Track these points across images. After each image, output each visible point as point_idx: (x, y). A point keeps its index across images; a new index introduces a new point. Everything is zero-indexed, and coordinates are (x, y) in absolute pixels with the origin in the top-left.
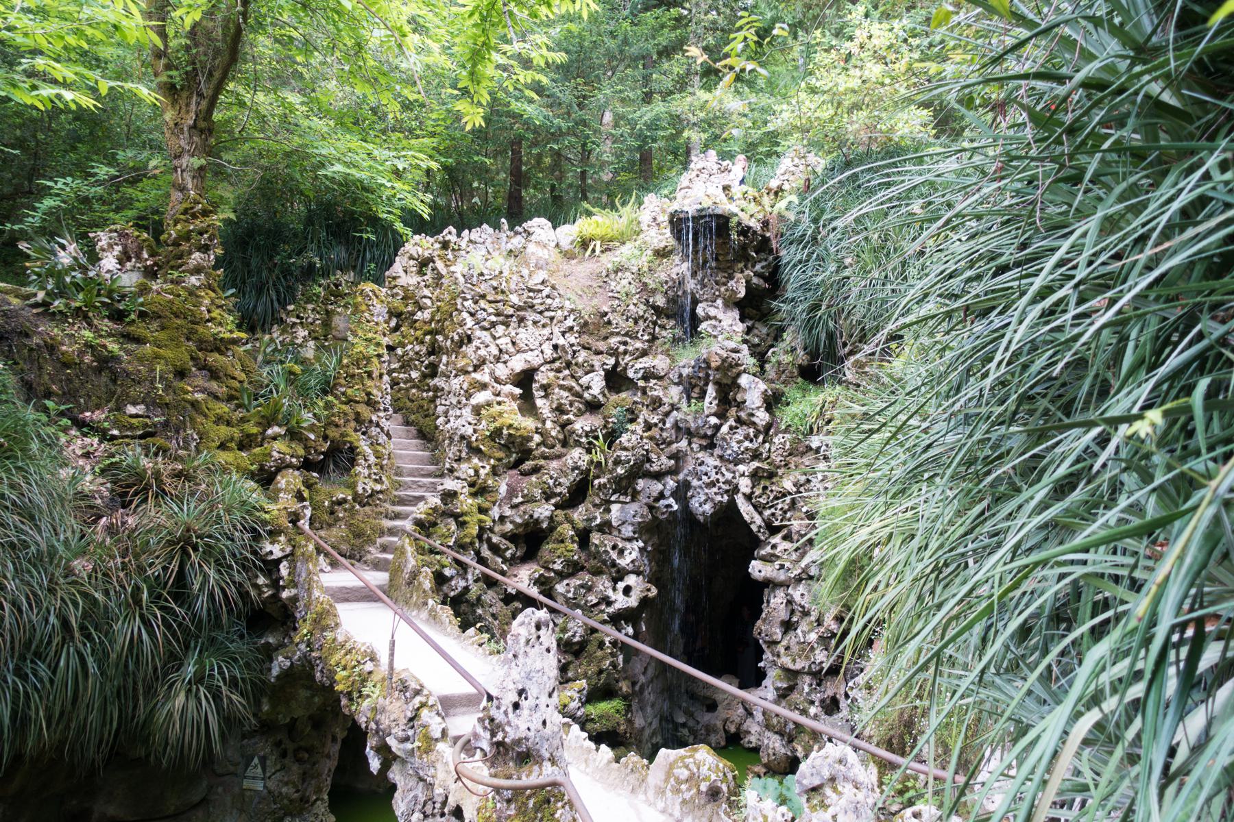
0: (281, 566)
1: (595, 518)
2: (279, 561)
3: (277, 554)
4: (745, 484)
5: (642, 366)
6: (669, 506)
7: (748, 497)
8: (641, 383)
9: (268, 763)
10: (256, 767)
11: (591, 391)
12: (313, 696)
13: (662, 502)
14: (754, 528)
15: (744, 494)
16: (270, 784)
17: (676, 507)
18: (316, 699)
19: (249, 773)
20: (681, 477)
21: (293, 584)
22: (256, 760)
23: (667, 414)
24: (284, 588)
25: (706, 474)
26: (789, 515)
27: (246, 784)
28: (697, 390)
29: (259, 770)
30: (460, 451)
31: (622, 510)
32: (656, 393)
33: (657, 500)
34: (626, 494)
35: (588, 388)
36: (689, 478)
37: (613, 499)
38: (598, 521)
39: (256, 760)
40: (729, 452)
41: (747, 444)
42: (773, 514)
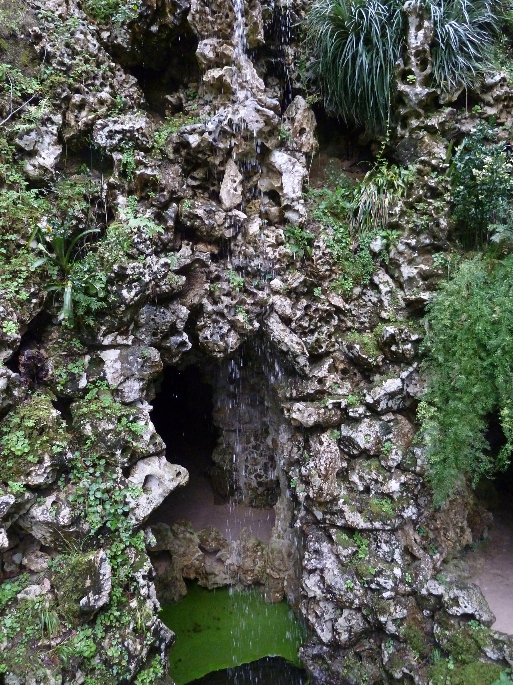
4: (283, 305)
6: (183, 344)
7: (286, 320)
11: (38, 161)
13: (175, 339)
17: (190, 345)
20: (193, 298)
23: (165, 206)
25: (227, 295)
26: (333, 340)
28: (199, 174)
31: (122, 358)
32: (149, 172)
35: (33, 154)
36: (205, 301)
42: (317, 340)
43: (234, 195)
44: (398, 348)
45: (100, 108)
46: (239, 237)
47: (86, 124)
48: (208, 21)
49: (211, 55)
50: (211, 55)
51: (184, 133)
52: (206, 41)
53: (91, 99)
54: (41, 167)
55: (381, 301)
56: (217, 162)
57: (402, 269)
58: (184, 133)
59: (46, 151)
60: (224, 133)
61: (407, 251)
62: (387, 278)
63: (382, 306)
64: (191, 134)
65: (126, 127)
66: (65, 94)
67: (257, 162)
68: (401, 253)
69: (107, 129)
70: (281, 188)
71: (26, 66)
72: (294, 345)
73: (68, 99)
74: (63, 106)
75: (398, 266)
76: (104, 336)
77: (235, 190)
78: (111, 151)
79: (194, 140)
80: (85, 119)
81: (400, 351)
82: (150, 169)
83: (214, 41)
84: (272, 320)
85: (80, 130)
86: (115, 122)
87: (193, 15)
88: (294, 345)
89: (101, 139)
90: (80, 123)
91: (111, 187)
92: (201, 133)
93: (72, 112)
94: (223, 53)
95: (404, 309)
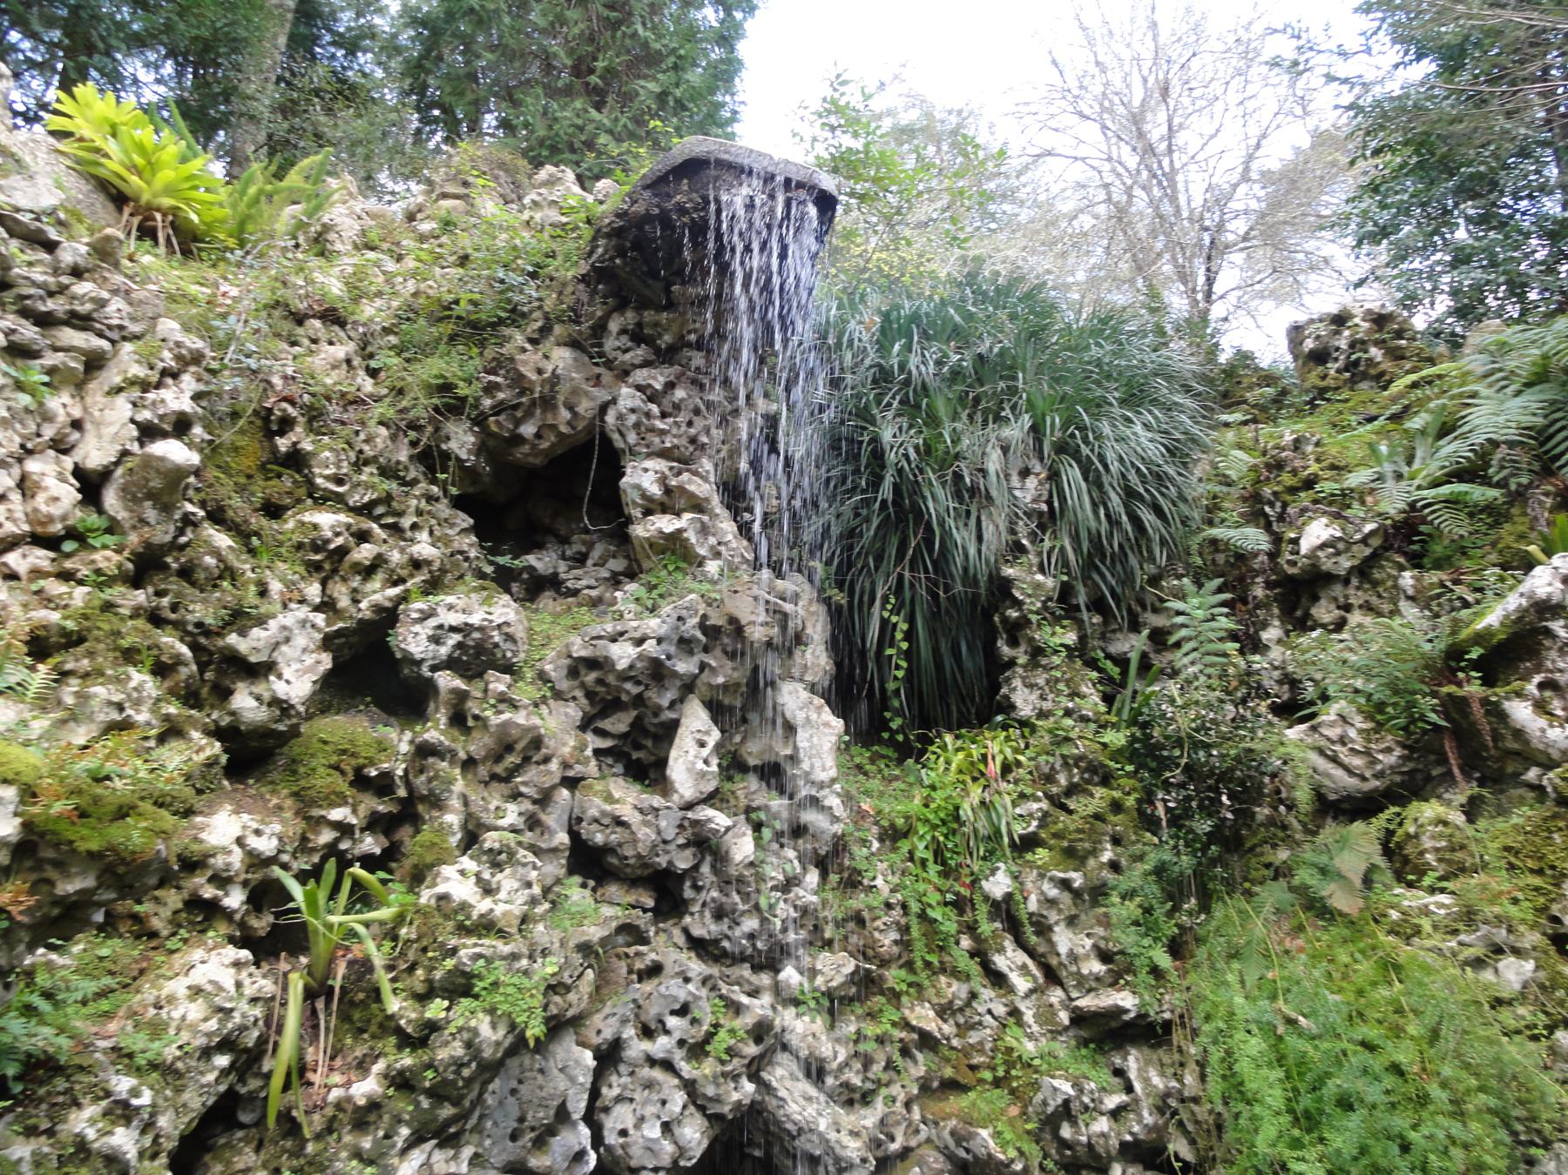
5: (454, 619)
8: (447, 681)
25: (683, 1011)
32: (520, 718)
43: (703, 775)
44: (1078, 1133)
45: (412, 576)
46: (705, 869)
47: (378, 609)
48: (652, 430)
49: (655, 490)
50: (655, 490)
51: (599, 637)
52: (649, 464)
53: (395, 557)
54: (275, 702)
55: (1015, 1013)
56: (665, 703)
57: (1055, 938)
58: (599, 637)
59: (295, 666)
60: (685, 644)
61: (1066, 898)
62: (1022, 957)
63: (1020, 1023)
64: (614, 640)
65: (475, 619)
66: (340, 541)
67: (742, 707)
68: (1052, 902)
69: (433, 622)
70: (793, 759)
71: (249, 477)
72: (846, 1139)
73: (343, 551)
74: (327, 566)
75: (1044, 930)
76: (404, 1152)
77: (706, 762)
78: (434, 669)
79: (623, 654)
80: (377, 597)
81: (1084, 1139)
82: (523, 713)
83: (661, 465)
84: (779, 1072)
85: (361, 621)
86: (450, 607)
87: (620, 417)
88: (846, 1139)
89: (414, 640)
90: (363, 605)
91: (424, 751)
92: (640, 642)
93: (344, 579)
94: (682, 489)
95: (1066, 1029)
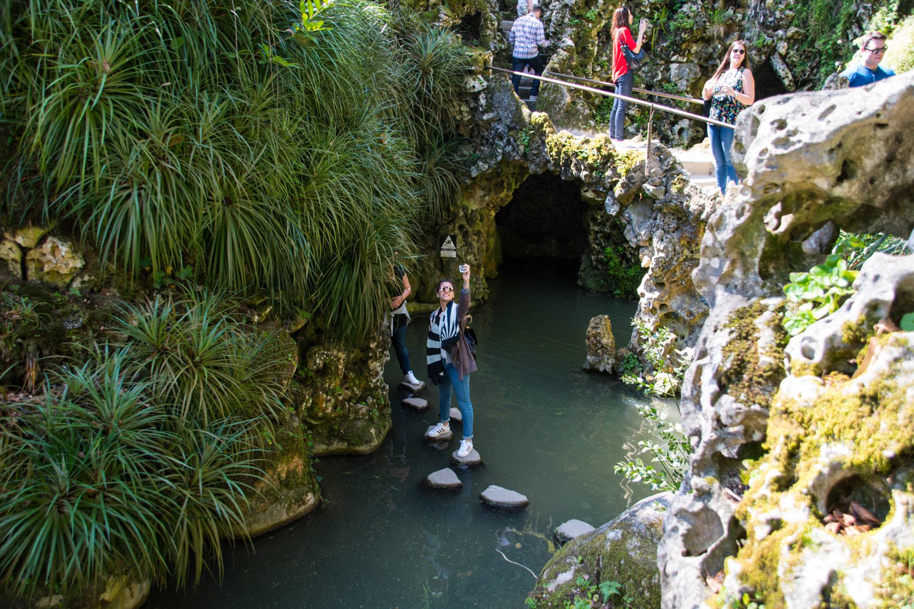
0: (480, 97)
1: (657, 75)
2: (479, 93)
3: (478, 87)
4: (782, 47)
7: (783, 58)
9: (457, 240)
10: (449, 242)
12: (485, 195)
14: (786, 82)
15: (780, 55)
16: (460, 253)
18: (487, 198)
19: (444, 246)
21: (489, 108)
22: (449, 238)
24: (483, 113)
27: (443, 254)
29: (452, 244)
30: (563, 18)
31: (679, 68)
33: (707, 60)
34: (683, 56)
37: (673, 59)
38: (660, 77)
39: (449, 238)
40: (770, 19)
41: (788, 12)
